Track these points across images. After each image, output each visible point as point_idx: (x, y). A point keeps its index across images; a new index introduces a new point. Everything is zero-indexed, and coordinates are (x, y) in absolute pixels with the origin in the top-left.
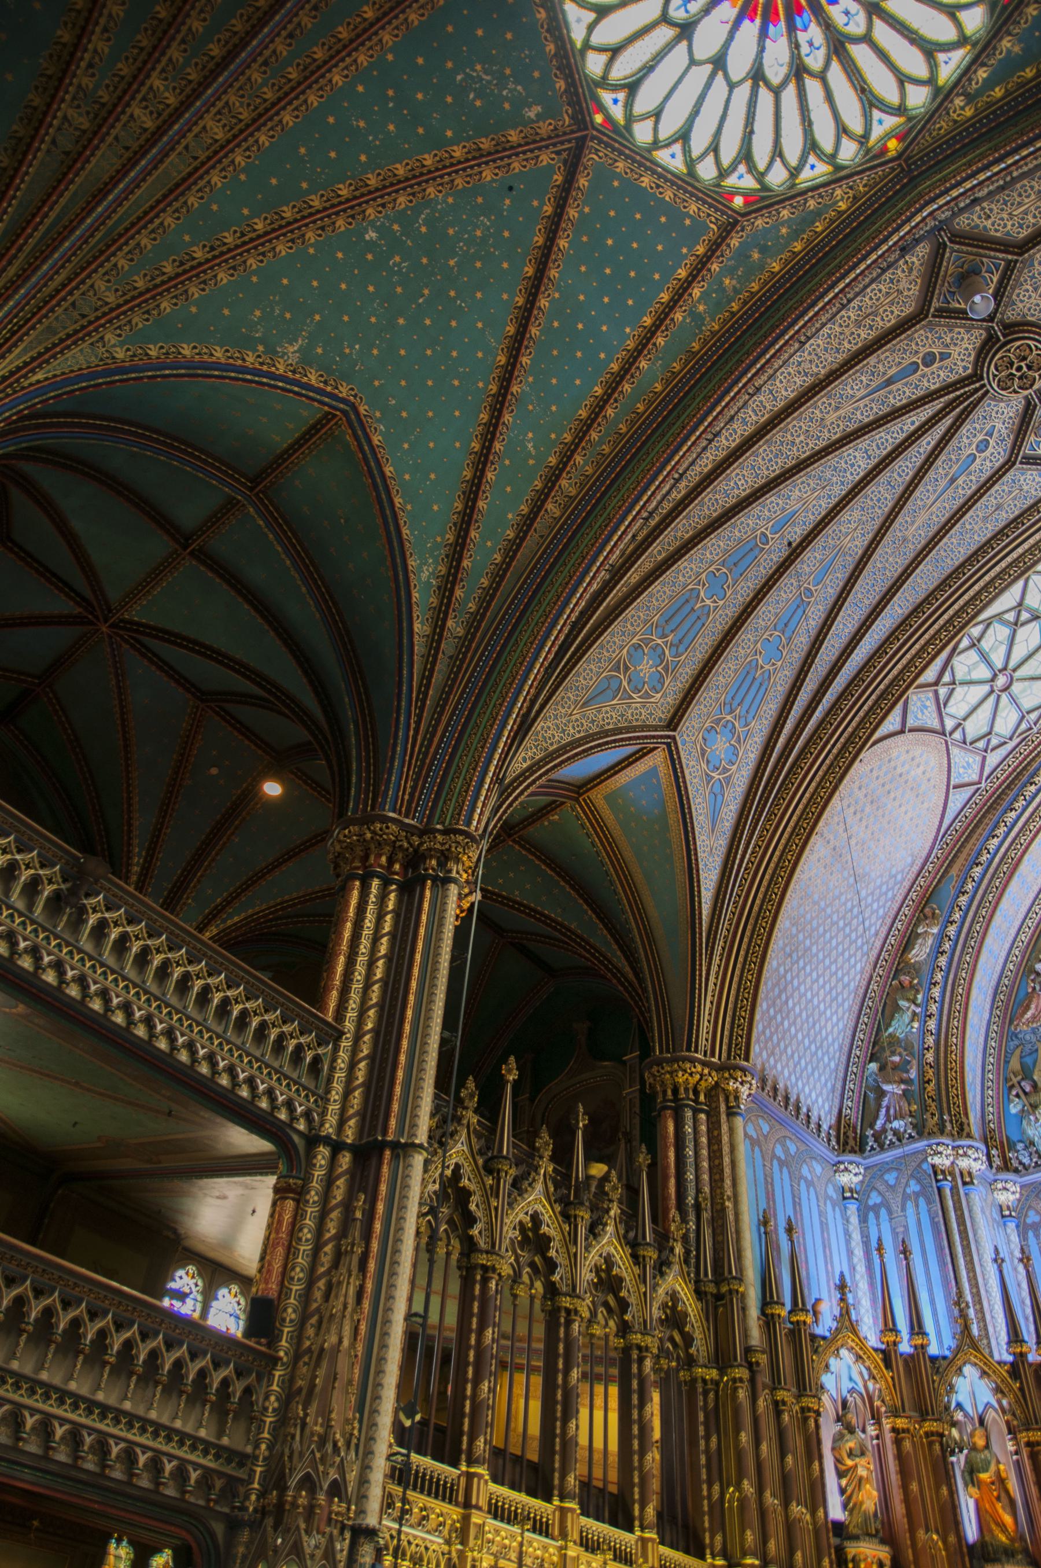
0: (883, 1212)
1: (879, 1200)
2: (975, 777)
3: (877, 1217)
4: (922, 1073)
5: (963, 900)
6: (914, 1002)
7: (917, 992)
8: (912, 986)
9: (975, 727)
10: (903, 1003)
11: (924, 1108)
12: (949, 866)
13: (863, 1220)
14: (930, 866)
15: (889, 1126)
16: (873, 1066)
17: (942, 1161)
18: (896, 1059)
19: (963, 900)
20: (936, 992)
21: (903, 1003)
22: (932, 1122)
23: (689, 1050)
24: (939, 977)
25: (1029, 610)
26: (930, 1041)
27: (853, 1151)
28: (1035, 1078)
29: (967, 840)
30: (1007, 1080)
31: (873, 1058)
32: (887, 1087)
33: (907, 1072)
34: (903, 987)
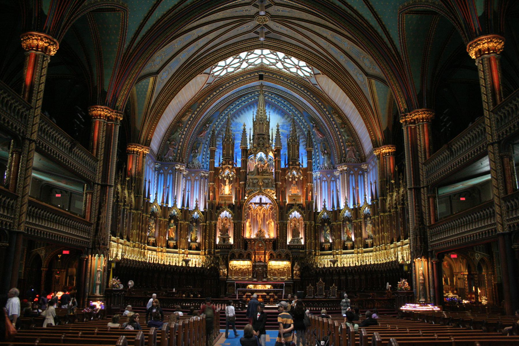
0: (163, 175)
2: (211, 82)
3: (161, 175)
4: (178, 147)
5: (198, 109)
6: (181, 130)
7: (182, 128)
8: (181, 127)
9: (216, 74)
11: (177, 156)
12: (198, 100)
13: (158, 175)
14: (194, 99)
19: (198, 109)
20: (186, 129)
21: (179, 130)
22: (178, 158)
23: (139, 143)
24: (188, 126)
25: (240, 56)
26: (182, 140)
27: (159, 160)
29: (204, 96)
30: (193, 148)
31: (169, 140)
33: (175, 146)
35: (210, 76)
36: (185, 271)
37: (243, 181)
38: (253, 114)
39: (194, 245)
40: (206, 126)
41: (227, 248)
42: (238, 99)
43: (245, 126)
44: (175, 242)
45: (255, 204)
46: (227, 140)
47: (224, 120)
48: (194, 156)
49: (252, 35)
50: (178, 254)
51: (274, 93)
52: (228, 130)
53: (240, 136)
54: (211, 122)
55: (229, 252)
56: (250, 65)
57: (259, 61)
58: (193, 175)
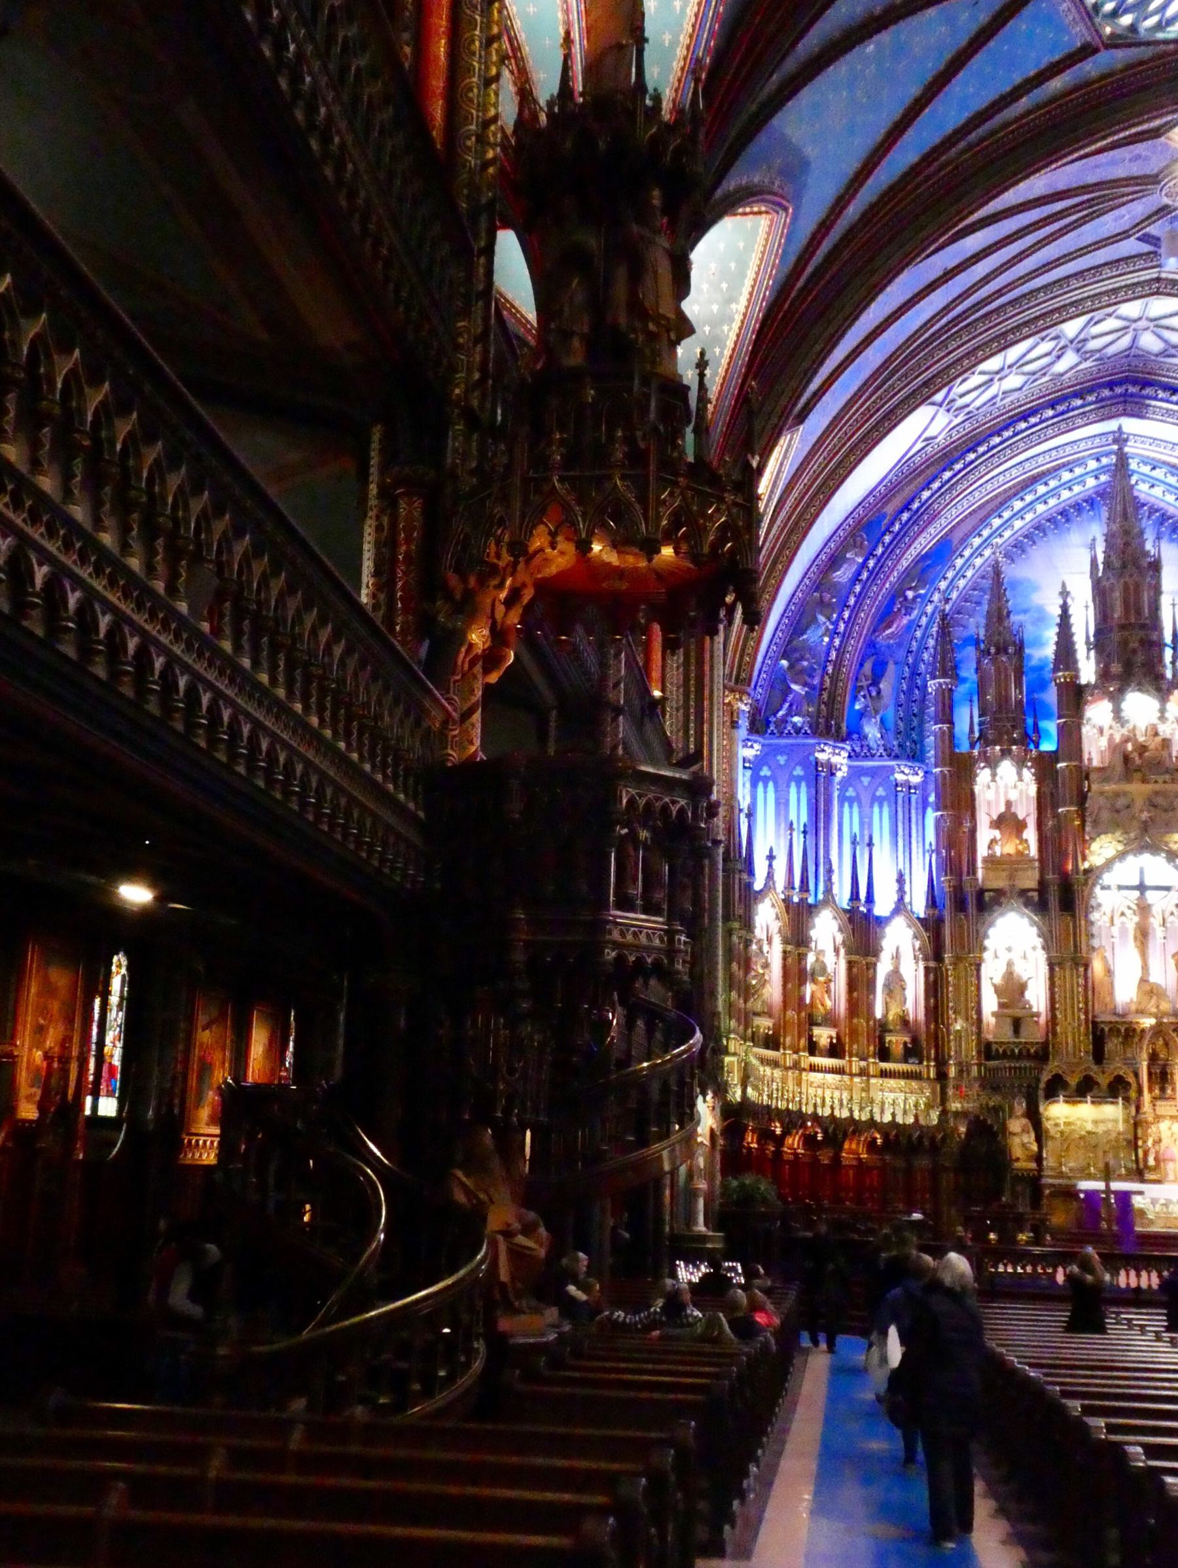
0: (771, 785)
1: (768, 773)
3: (765, 787)
4: (822, 682)
6: (829, 619)
8: (830, 605)
10: (821, 619)
11: (819, 711)
13: (754, 785)
15: (789, 719)
16: (784, 663)
17: (822, 757)
18: (805, 663)
20: (846, 615)
21: (821, 619)
26: (833, 655)
27: (757, 732)
28: (881, 686)
31: (785, 656)
32: (794, 687)
33: (811, 676)
34: (821, 601)
35: (942, 410)
36: (926, 1143)
37: (1071, 804)
38: (1092, 547)
39: (896, 1041)
40: (906, 598)
41: (1029, 1056)
42: (1023, 489)
43: (1068, 593)
44: (833, 1033)
45: (1120, 888)
46: (998, 652)
47: (969, 574)
48: (866, 706)
49: (1130, 246)
50: (846, 1078)
51: (1165, 463)
52: (999, 615)
53: (1051, 635)
54: (922, 582)
55: (1041, 1070)
56: (1086, 360)
57: (1125, 342)
58: (866, 780)
